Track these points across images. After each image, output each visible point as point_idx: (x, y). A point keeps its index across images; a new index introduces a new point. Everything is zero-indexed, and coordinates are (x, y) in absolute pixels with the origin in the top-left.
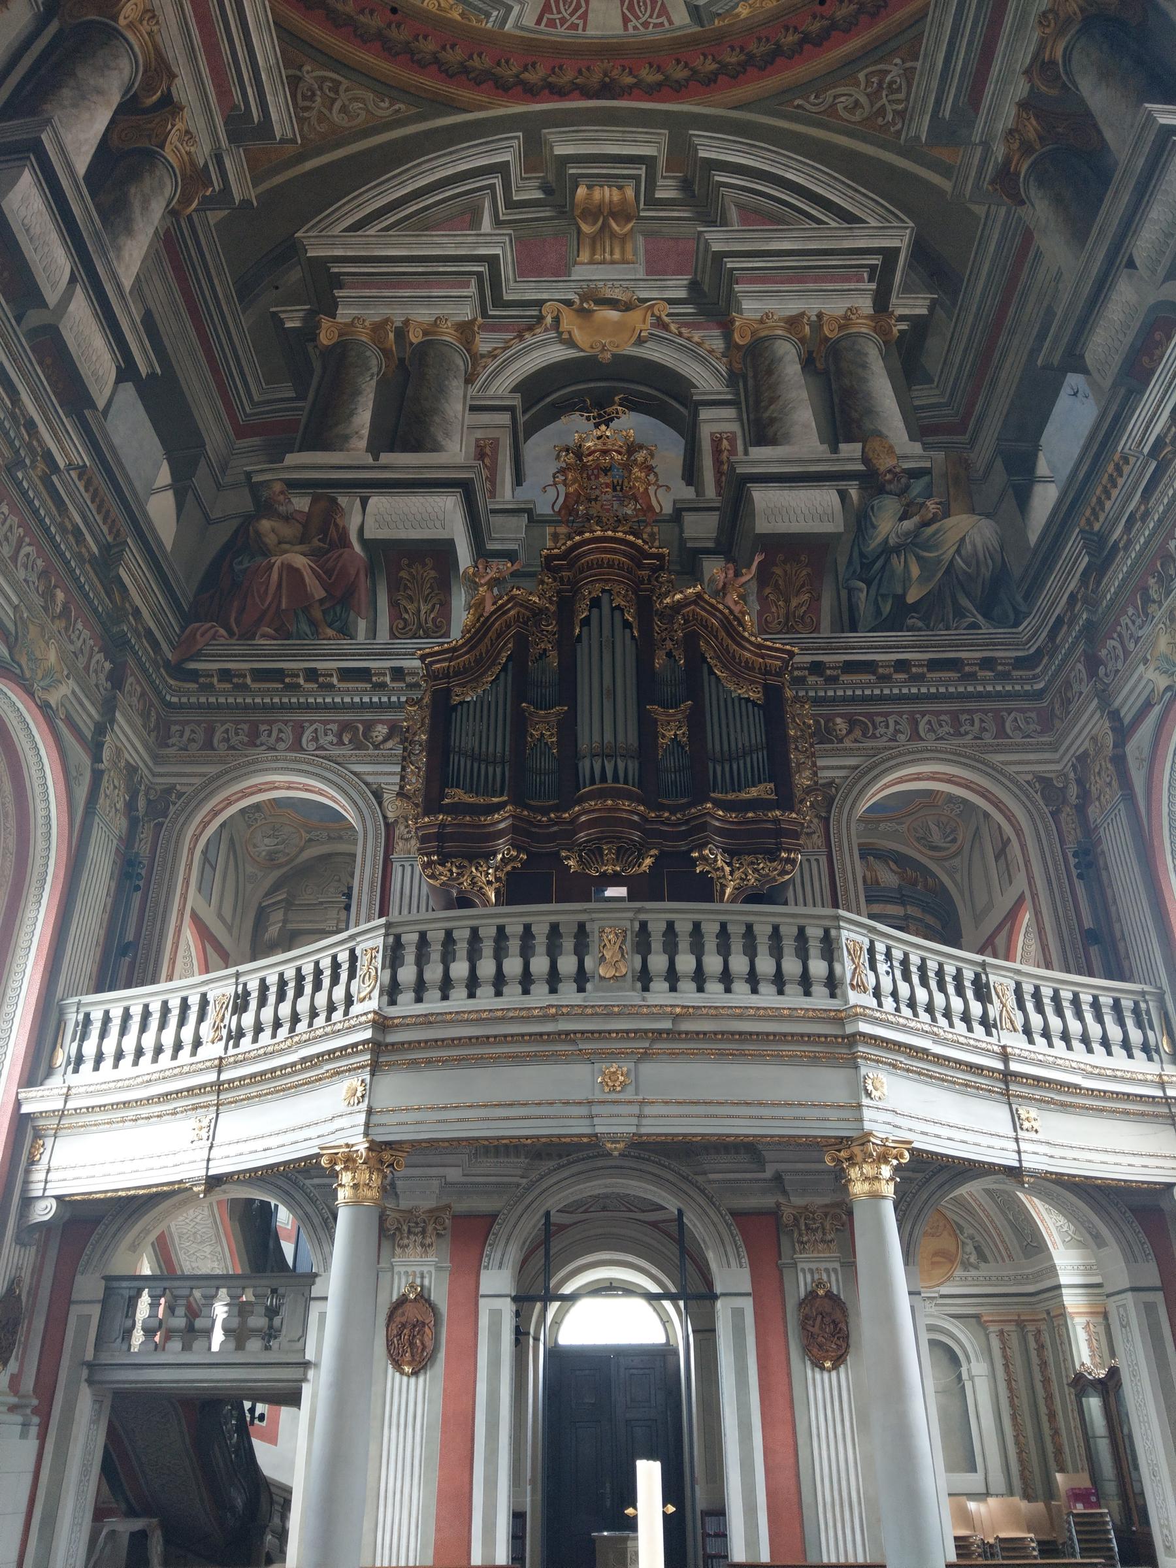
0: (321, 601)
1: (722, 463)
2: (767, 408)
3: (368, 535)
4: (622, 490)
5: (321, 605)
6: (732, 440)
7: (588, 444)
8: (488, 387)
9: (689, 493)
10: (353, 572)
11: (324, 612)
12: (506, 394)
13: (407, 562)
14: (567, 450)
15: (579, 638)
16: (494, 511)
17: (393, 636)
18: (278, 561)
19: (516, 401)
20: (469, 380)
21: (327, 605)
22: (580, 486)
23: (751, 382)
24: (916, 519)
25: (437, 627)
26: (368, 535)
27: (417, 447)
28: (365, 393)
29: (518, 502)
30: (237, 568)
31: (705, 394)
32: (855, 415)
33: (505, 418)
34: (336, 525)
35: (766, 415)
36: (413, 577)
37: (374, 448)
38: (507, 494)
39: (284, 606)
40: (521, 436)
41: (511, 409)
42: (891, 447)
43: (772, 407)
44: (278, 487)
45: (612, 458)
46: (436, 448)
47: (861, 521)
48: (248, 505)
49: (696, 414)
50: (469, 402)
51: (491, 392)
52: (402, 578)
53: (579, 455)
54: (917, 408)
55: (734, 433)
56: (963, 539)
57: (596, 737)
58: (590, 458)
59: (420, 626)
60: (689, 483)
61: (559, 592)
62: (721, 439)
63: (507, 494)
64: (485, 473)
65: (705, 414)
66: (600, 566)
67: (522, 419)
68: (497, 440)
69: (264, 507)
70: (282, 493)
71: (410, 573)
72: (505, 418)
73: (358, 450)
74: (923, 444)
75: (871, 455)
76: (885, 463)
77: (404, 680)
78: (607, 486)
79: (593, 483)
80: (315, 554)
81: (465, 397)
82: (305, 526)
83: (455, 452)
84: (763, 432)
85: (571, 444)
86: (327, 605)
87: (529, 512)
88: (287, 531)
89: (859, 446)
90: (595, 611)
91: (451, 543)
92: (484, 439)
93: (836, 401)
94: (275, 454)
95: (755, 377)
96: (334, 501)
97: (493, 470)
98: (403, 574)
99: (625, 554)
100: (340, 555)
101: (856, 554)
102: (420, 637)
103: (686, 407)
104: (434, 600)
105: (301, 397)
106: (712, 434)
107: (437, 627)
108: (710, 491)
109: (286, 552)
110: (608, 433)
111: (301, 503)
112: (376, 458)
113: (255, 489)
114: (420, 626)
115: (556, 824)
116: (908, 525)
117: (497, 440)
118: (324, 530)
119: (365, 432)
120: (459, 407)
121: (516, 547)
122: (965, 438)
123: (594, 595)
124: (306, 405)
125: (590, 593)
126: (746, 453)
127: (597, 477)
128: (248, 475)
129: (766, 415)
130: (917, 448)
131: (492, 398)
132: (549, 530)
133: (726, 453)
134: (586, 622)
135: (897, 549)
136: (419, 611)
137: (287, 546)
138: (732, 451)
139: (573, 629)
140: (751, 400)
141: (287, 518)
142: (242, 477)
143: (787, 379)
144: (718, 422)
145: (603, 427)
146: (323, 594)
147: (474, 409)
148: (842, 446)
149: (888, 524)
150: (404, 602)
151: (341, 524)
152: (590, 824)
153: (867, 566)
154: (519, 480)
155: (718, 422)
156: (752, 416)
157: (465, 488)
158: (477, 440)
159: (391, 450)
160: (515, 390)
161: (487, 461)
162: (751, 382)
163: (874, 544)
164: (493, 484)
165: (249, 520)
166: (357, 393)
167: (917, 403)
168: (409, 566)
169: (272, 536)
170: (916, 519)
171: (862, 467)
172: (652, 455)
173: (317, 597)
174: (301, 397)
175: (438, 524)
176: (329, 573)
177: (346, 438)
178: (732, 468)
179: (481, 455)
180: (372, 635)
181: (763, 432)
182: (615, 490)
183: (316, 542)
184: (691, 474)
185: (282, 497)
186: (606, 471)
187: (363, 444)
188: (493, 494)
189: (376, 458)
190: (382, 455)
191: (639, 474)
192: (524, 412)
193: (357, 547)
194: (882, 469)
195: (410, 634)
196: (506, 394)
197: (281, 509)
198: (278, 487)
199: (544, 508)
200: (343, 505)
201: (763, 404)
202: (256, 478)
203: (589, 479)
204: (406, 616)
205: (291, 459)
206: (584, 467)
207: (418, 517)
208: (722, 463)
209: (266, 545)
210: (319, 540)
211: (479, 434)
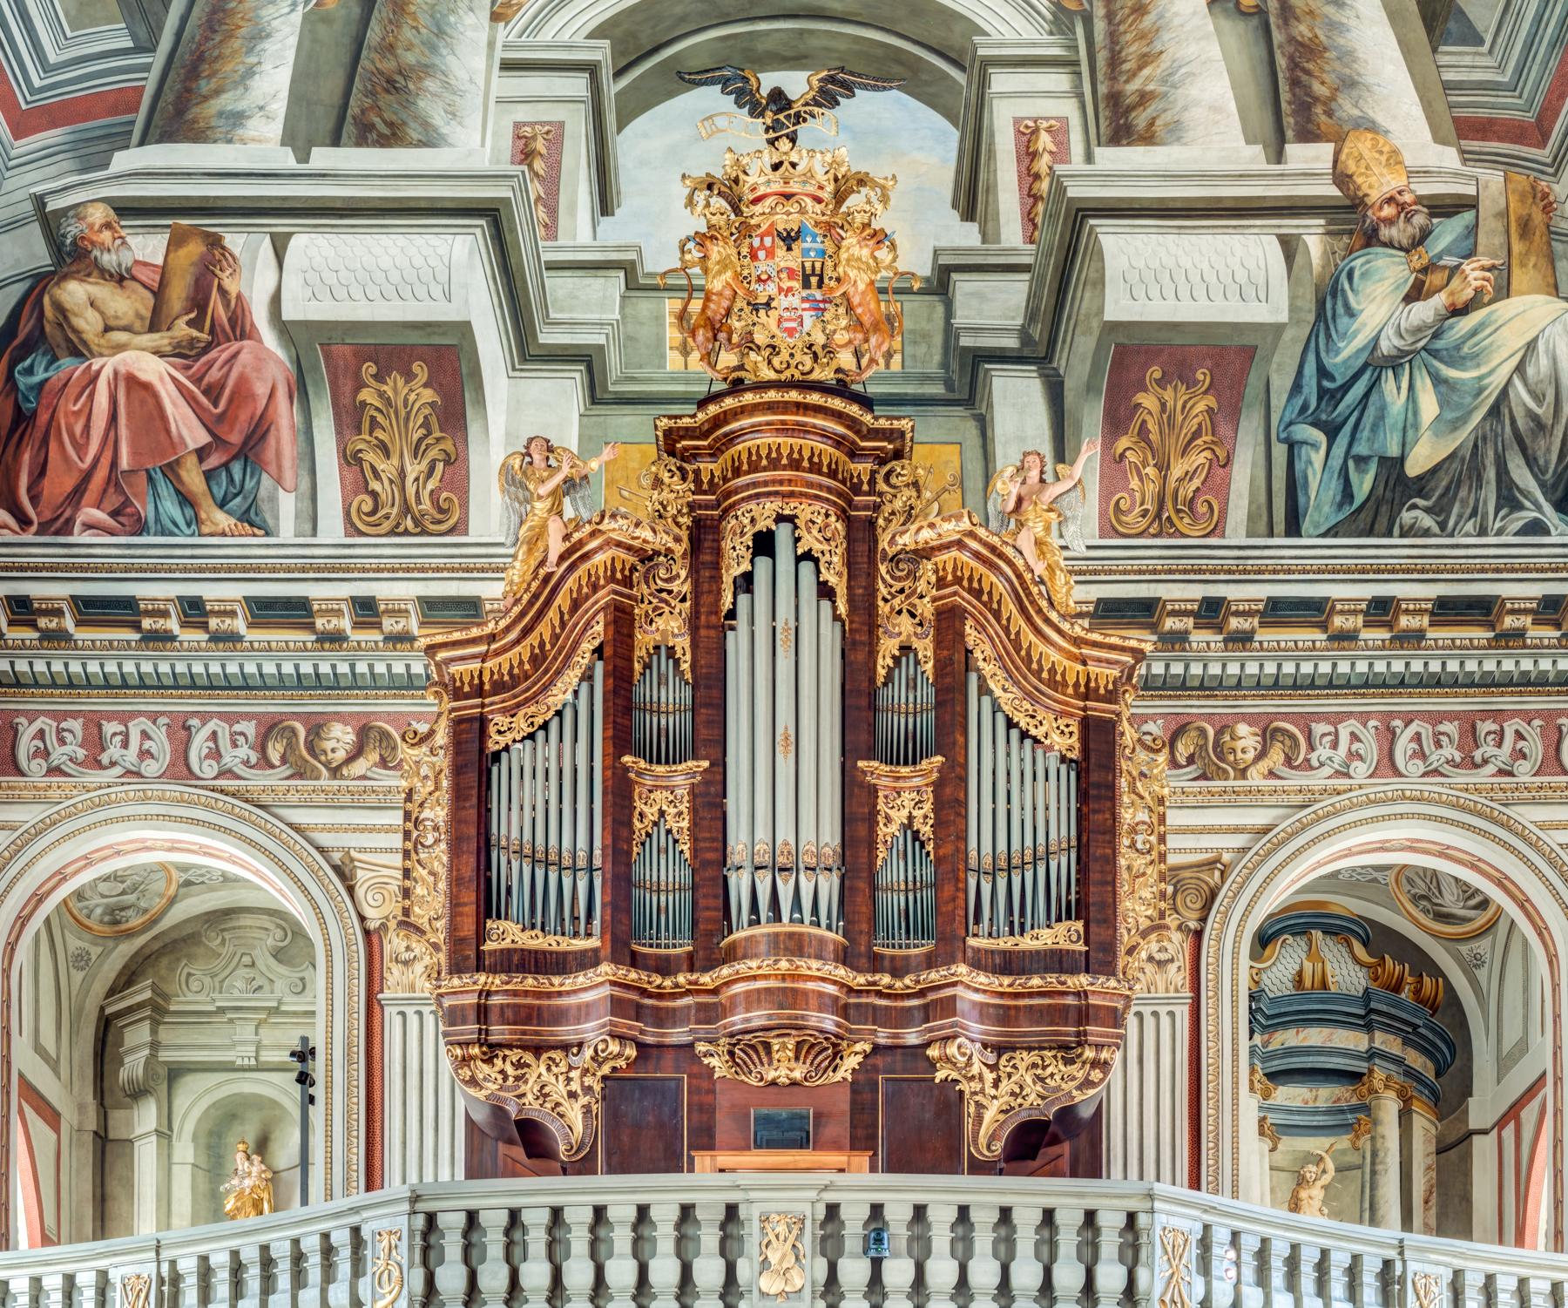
0: (202, 454)
1: (1037, 177)
2: (1133, 74)
3: (288, 314)
4: (820, 284)
5: (201, 460)
6: (1059, 132)
7: (751, 180)
8: (539, 28)
9: (967, 236)
10: (261, 390)
11: (209, 475)
12: (579, 39)
13: (373, 370)
14: (710, 187)
15: (732, 614)
16: (553, 266)
17: (352, 529)
18: (107, 366)
19: (601, 52)
20: (495, 17)
21: (214, 461)
22: (737, 275)
23: (1100, 26)
24: (1439, 301)
25: (441, 511)
26: (288, 314)
27: (392, 136)
28: (278, 36)
29: (604, 249)
30: (23, 381)
31: (1001, 45)
32: (1319, 89)
33: (578, 85)
34: (223, 292)
35: (1132, 87)
36: (388, 402)
37: (298, 138)
38: (579, 229)
39: (124, 463)
40: (611, 119)
41: (591, 69)
42: (1395, 152)
43: (1146, 72)
44: (98, 214)
45: (802, 211)
46: (430, 139)
47: (1328, 303)
48: (38, 254)
49: (983, 83)
50: (499, 54)
51: (547, 35)
52: (364, 404)
53: (729, 190)
54: (1448, 86)
55: (1064, 121)
56: (1531, 346)
57: (762, 833)
58: (758, 209)
59: (406, 509)
60: (969, 214)
61: (692, 506)
62: (1036, 131)
63: (579, 229)
64: (535, 189)
65: (1001, 81)
66: (774, 464)
67: (612, 89)
68: (561, 124)
69: (72, 256)
70: (108, 226)
71: (381, 394)
72: (578, 85)
73: (267, 140)
74: (1462, 152)
75: (1351, 167)
76: (1378, 183)
77: (378, 626)
78: (791, 273)
79: (763, 266)
80: (184, 353)
81: (491, 45)
82: (159, 293)
83: (470, 136)
84: (1121, 120)
85: (718, 174)
86: (214, 461)
87: (629, 269)
88: (126, 304)
89: (1327, 149)
90: (763, 563)
91: (465, 329)
92: (532, 124)
93: (1282, 62)
94: (92, 155)
95: (1110, 16)
96: (215, 242)
97: (552, 182)
98: (366, 395)
99: (824, 435)
100: (235, 356)
101: (1310, 369)
102: (406, 533)
103: (962, 68)
104: (433, 453)
105: (145, 46)
106: (1017, 121)
107: (441, 511)
108: (1012, 232)
109: (120, 348)
110: (794, 157)
111: (147, 246)
112: (304, 157)
113: (50, 222)
114: (406, 509)
115: (688, 992)
116: (1424, 311)
117: (561, 124)
118: (198, 302)
119: (280, 107)
120: (479, 63)
121: (602, 340)
122: (1544, 155)
123: (762, 525)
124: (158, 60)
125: (753, 520)
126: (1089, 158)
127: (770, 254)
128: (39, 201)
129: (1132, 87)
130: (1449, 157)
131: (548, 47)
132: (672, 305)
133: (1046, 158)
134: (746, 582)
135: (1394, 363)
136: (402, 474)
137: (121, 337)
138: (1062, 154)
139: (719, 593)
140: (1102, 57)
141: (120, 279)
142: (28, 207)
143: (1177, 21)
144: (1029, 100)
145: (784, 145)
146: (204, 438)
147: (508, 66)
148: (1292, 149)
149: (1379, 308)
150: (370, 457)
151: (232, 286)
152: (753, 999)
153: (1330, 396)
154: (605, 203)
155: (1029, 100)
156: (1103, 89)
157: (493, 215)
158: (517, 125)
159: (336, 141)
160: (598, 33)
161: (539, 165)
162: (1100, 26)
163: (1346, 352)
164: (553, 211)
165: (40, 283)
166: (260, 35)
167: (1449, 76)
168: (379, 377)
169: (91, 315)
170: (1439, 301)
171: (1334, 191)
172: (885, 199)
173: (192, 446)
174: (145, 46)
175: (437, 292)
176: (213, 392)
177: (238, 118)
178: (1059, 188)
179: (526, 155)
180: (308, 527)
181: (1121, 120)
182: (806, 284)
183: (182, 329)
184: (971, 198)
185: (106, 236)
186: (789, 239)
187: (275, 129)
188: (551, 230)
189: (304, 157)
190: (314, 150)
191: (856, 251)
192: (618, 74)
193: (269, 338)
194: (1375, 196)
195: (387, 526)
196: (579, 39)
197: (108, 260)
198: (98, 214)
199: (660, 259)
200: (236, 252)
201: (1126, 67)
202: (53, 205)
203: (754, 256)
204: (375, 485)
205: (123, 161)
206: (745, 230)
207: (395, 277)
208: (1037, 177)
209: (76, 331)
210: (190, 323)
211: (523, 114)
